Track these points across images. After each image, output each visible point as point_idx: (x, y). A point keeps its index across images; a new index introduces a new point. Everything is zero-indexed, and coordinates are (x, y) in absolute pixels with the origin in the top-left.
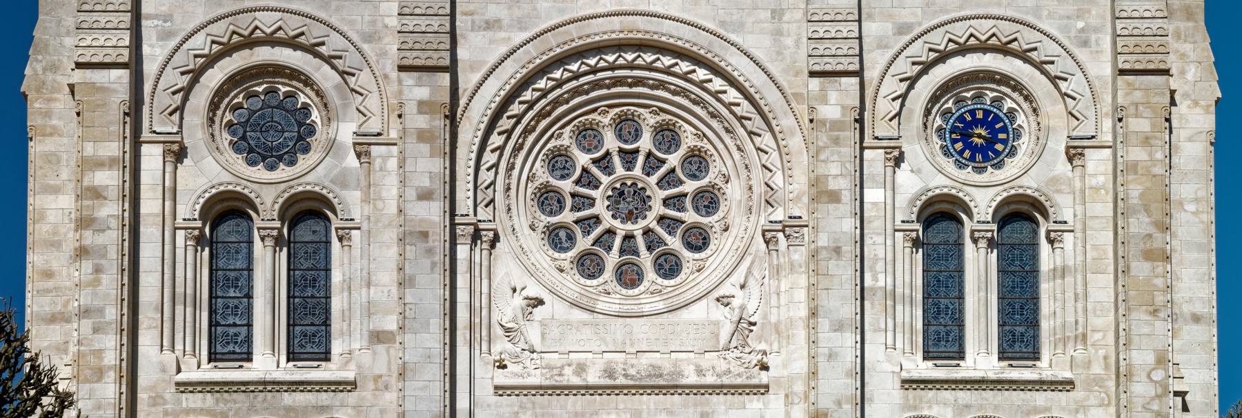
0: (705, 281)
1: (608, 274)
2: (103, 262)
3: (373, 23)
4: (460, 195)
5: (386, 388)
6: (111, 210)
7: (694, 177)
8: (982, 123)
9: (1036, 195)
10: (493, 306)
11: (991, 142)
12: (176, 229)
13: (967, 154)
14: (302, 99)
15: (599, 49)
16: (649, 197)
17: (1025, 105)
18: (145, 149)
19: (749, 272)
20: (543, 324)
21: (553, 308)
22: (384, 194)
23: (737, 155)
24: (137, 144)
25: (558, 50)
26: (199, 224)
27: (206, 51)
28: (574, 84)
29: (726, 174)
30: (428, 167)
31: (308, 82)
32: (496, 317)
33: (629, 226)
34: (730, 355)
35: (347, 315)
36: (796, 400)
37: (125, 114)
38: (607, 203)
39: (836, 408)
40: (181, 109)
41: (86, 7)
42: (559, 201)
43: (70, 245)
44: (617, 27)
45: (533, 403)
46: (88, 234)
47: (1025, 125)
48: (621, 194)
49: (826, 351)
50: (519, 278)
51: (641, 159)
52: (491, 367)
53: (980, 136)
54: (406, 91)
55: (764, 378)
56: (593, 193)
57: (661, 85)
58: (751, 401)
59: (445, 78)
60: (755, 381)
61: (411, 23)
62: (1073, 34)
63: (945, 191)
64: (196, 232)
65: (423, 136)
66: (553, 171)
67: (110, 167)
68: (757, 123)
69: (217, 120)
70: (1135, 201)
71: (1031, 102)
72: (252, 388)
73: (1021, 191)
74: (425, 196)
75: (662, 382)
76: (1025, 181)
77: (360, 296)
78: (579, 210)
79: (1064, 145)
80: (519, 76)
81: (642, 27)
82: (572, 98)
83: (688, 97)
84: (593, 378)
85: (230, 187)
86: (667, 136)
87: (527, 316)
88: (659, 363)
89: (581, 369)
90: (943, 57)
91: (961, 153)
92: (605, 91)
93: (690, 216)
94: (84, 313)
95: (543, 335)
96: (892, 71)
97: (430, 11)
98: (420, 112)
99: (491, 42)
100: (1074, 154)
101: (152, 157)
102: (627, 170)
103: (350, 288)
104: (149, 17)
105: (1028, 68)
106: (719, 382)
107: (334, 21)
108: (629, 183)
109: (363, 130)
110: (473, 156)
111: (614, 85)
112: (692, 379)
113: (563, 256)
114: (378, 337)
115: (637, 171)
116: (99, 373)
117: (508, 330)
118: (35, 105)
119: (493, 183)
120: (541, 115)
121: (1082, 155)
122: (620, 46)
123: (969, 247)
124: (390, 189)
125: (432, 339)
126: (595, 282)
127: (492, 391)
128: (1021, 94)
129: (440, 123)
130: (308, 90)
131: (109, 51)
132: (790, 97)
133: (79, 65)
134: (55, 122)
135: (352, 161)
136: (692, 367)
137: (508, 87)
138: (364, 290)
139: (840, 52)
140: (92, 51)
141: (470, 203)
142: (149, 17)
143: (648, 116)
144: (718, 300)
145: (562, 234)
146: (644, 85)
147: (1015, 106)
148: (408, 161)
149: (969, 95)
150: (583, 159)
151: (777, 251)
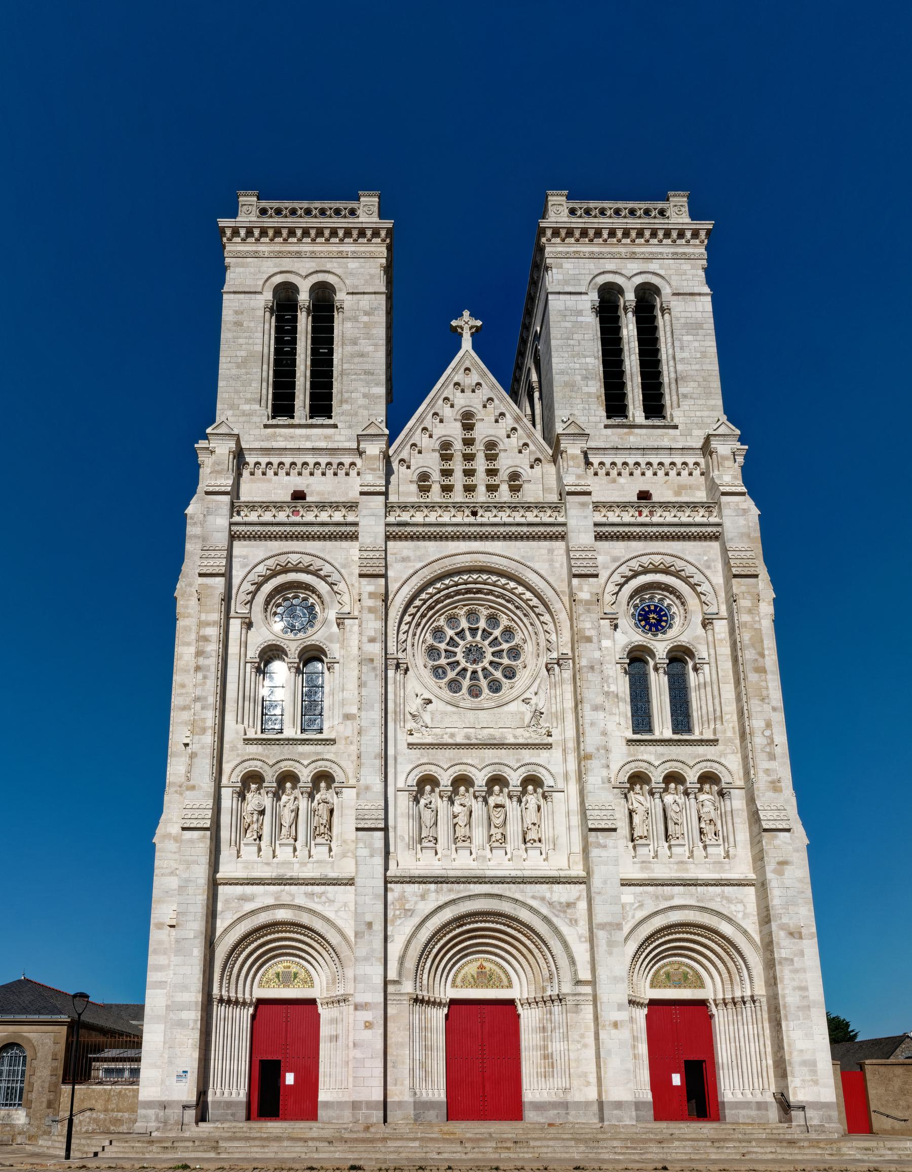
0: (515, 692)
1: (464, 690)
2: (208, 673)
3: (347, 559)
4: (389, 644)
5: (351, 743)
6: (213, 647)
7: (507, 642)
8: (654, 611)
9: (688, 645)
10: (406, 704)
11: (659, 621)
12: (246, 662)
13: (647, 627)
14: (311, 600)
15: (459, 572)
16: (484, 652)
17: (677, 602)
18: (232, 621)
19: (539, 686)
20: (432, 713)
21: (437, 705)
22: (351, 644)
23: (530, 628)
24: (228, 618)
25: (439, 572)
26: (258, 660)
27: (264, 573)
28: (446, 592)
30: (373, 625)
31: (314, 590)
32: (408, 709)
33: (474, 666)
34: (530, 729)
35: (332, 708)
36: (570, 752)
37: (222, 600)
38: (463, 655)
39: (596, 752)
40: (250, 602)
41: (205, 548)
42: (438, 654)
43: (192, 665)
44: (469, 560)
45: (428, 753)
46: (201, 659)
47: (677, 612)
48: (470, 650)
49: (589, 721)
50: (420, 689)
51: (480, 632)
52: (405, 734)
53: (653, 618)
54: (363, 588)
55: (550, 740)
57: (490, 593)
58: (543, 753)
59: (383, 581)
60: (545, 742)
61: (365, 554)
62: (702, 563)
63: (640, 643)
64: (256, 665)
65: (371, 610)
67: (213, 626)
68: (541, 609)
69: (269, 610)
70: (747, 642)
71: (680, 599)
72: (282, 742)
73: (679, 643)
74: (372, 640)
75: (496, 742)
76: (682, 638)
77: (339, 697)
79: (701, 618)
80: (419, 584)
81: (482, 560)
82: (445, 600)
83: (504, 599)
84: (459, 739)
85: (274, 642)
86: (493, 620)
87: (424, 709)
88: (493, 733)
89: (452, 735)
90: (636, 574)
91: (644, 627)
92: (461, 597)
93: (506, 661)
94: (197, 699)
95: (432, 718)
96: (611, 580)
97: (374, 549)
98: (370, 598)
99: (405, 567)
100: (706, 623)
101: (235, 625)
103: (333, 694)
104: (237, 557)
105: (679, 581)
106: (526, 742)
107: (327, 558)
108: (474, 645)
109: (341, 611)
110: (396, 625)
111: (466, 593)
112: (511, 740)
113: (441, 681)
114: (347, 717)
115: (478, 638)
116: (204, 731)
117: (414, 716)
118: (180, 603)
119: (406, 640)
120: (430, 608)
121: (711, 623)
122: (470, 571)
123: (653, 675)
124: (354, 642)
125: (376, 714)
126: (458, 695)
127: (406, 746)
128: (675, 595)
129: (379, 603)
130: (314, 596)
131: (215, 568)
132: (559, 593)
133: (201, 575)
134: (189, 611)
135: (335, 628)
136: (511, 735)
137: (414, 590)
138: (341, 693)
139: (588, 565)
140: (207, 568)
141: (395, 648)
142: (237, 557)
143: (483, 610)
144: (523, 701)
145: (440, 671)
146: (482, 593)
147: (671, 602)
148: (364, 623)
149: (647, 597)
150: (450, 633)
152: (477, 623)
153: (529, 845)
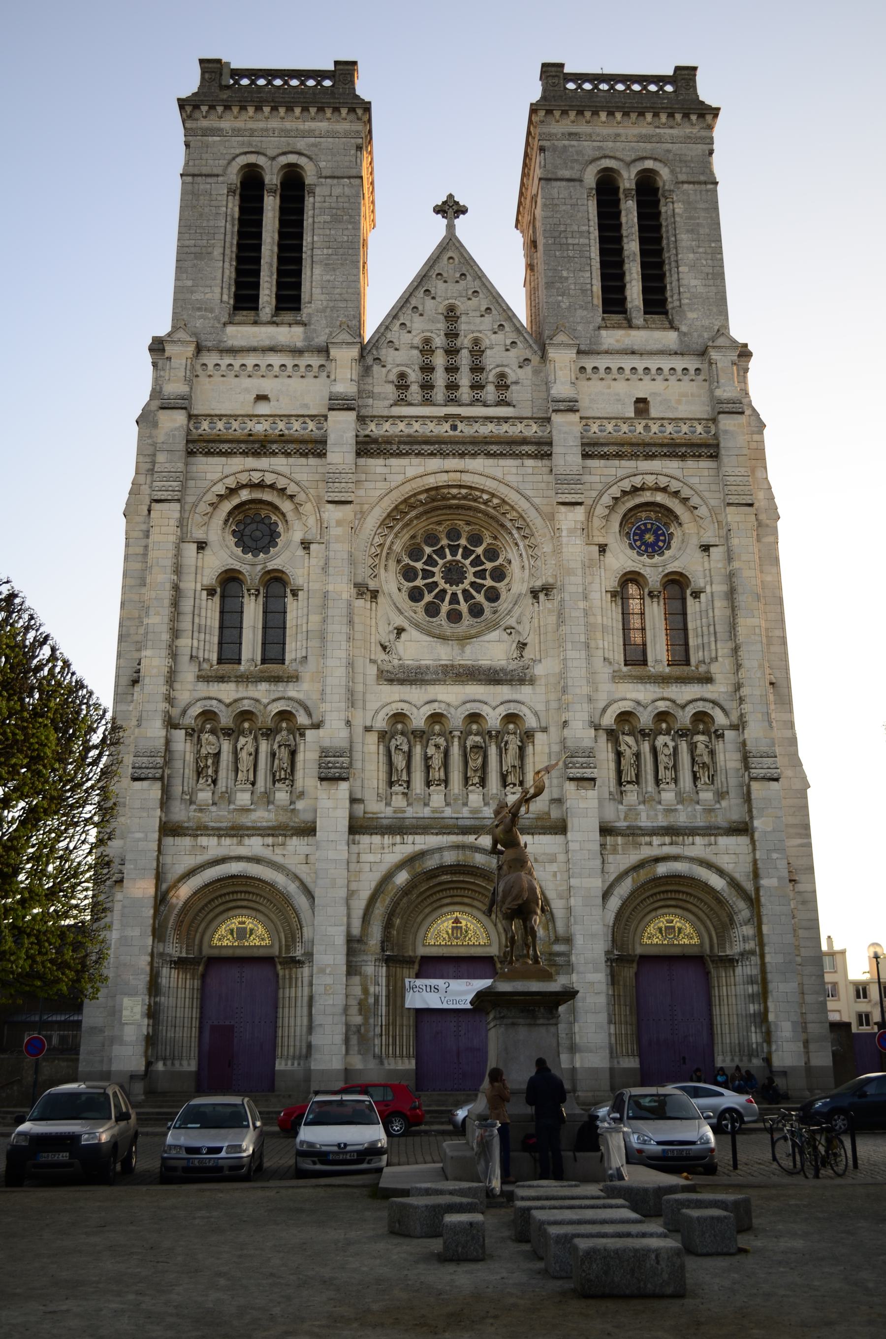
153: (508, 788)
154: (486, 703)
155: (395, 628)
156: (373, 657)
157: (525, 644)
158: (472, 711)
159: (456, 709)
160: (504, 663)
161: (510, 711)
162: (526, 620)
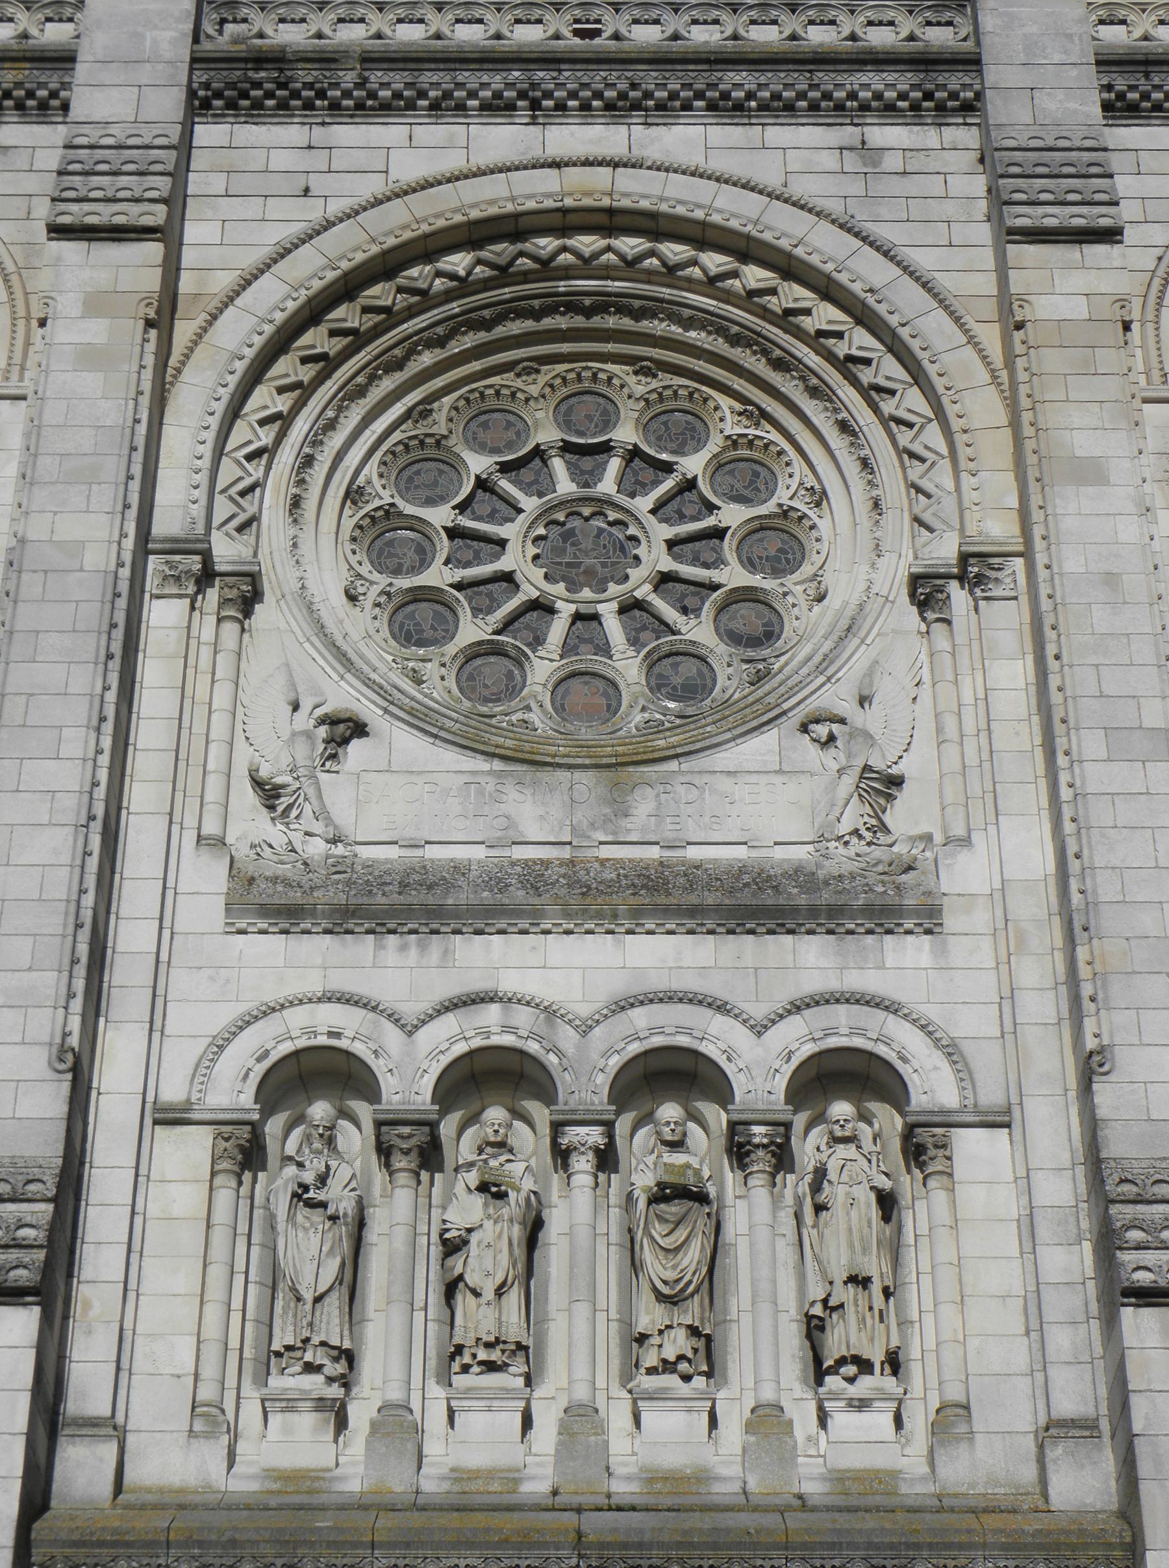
29: (817, 487)
38: (532, 550)
56: (505, 563)
66: (408, 489)
78: (467, 565)
102: (584, 487)
143: (632, 380)
151: (948, 622)
152: (603, 431)
153: (833, 1382)
154: (722, 1008)
155: (322, 721)
156: (211, 827)
157: (896, 782)
158: (658, 1041)
159: (585, 1029)
160: (801, 853)
161: (833, 1042)
162: (886, 690)
